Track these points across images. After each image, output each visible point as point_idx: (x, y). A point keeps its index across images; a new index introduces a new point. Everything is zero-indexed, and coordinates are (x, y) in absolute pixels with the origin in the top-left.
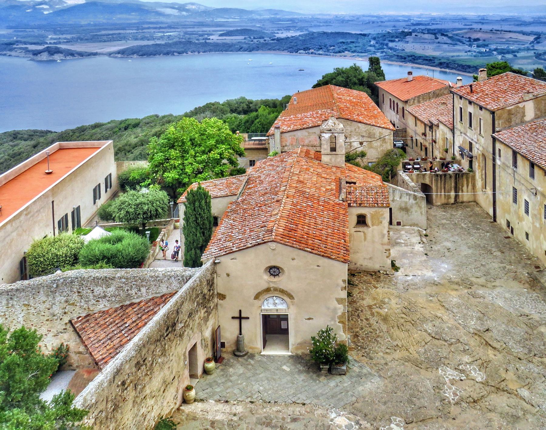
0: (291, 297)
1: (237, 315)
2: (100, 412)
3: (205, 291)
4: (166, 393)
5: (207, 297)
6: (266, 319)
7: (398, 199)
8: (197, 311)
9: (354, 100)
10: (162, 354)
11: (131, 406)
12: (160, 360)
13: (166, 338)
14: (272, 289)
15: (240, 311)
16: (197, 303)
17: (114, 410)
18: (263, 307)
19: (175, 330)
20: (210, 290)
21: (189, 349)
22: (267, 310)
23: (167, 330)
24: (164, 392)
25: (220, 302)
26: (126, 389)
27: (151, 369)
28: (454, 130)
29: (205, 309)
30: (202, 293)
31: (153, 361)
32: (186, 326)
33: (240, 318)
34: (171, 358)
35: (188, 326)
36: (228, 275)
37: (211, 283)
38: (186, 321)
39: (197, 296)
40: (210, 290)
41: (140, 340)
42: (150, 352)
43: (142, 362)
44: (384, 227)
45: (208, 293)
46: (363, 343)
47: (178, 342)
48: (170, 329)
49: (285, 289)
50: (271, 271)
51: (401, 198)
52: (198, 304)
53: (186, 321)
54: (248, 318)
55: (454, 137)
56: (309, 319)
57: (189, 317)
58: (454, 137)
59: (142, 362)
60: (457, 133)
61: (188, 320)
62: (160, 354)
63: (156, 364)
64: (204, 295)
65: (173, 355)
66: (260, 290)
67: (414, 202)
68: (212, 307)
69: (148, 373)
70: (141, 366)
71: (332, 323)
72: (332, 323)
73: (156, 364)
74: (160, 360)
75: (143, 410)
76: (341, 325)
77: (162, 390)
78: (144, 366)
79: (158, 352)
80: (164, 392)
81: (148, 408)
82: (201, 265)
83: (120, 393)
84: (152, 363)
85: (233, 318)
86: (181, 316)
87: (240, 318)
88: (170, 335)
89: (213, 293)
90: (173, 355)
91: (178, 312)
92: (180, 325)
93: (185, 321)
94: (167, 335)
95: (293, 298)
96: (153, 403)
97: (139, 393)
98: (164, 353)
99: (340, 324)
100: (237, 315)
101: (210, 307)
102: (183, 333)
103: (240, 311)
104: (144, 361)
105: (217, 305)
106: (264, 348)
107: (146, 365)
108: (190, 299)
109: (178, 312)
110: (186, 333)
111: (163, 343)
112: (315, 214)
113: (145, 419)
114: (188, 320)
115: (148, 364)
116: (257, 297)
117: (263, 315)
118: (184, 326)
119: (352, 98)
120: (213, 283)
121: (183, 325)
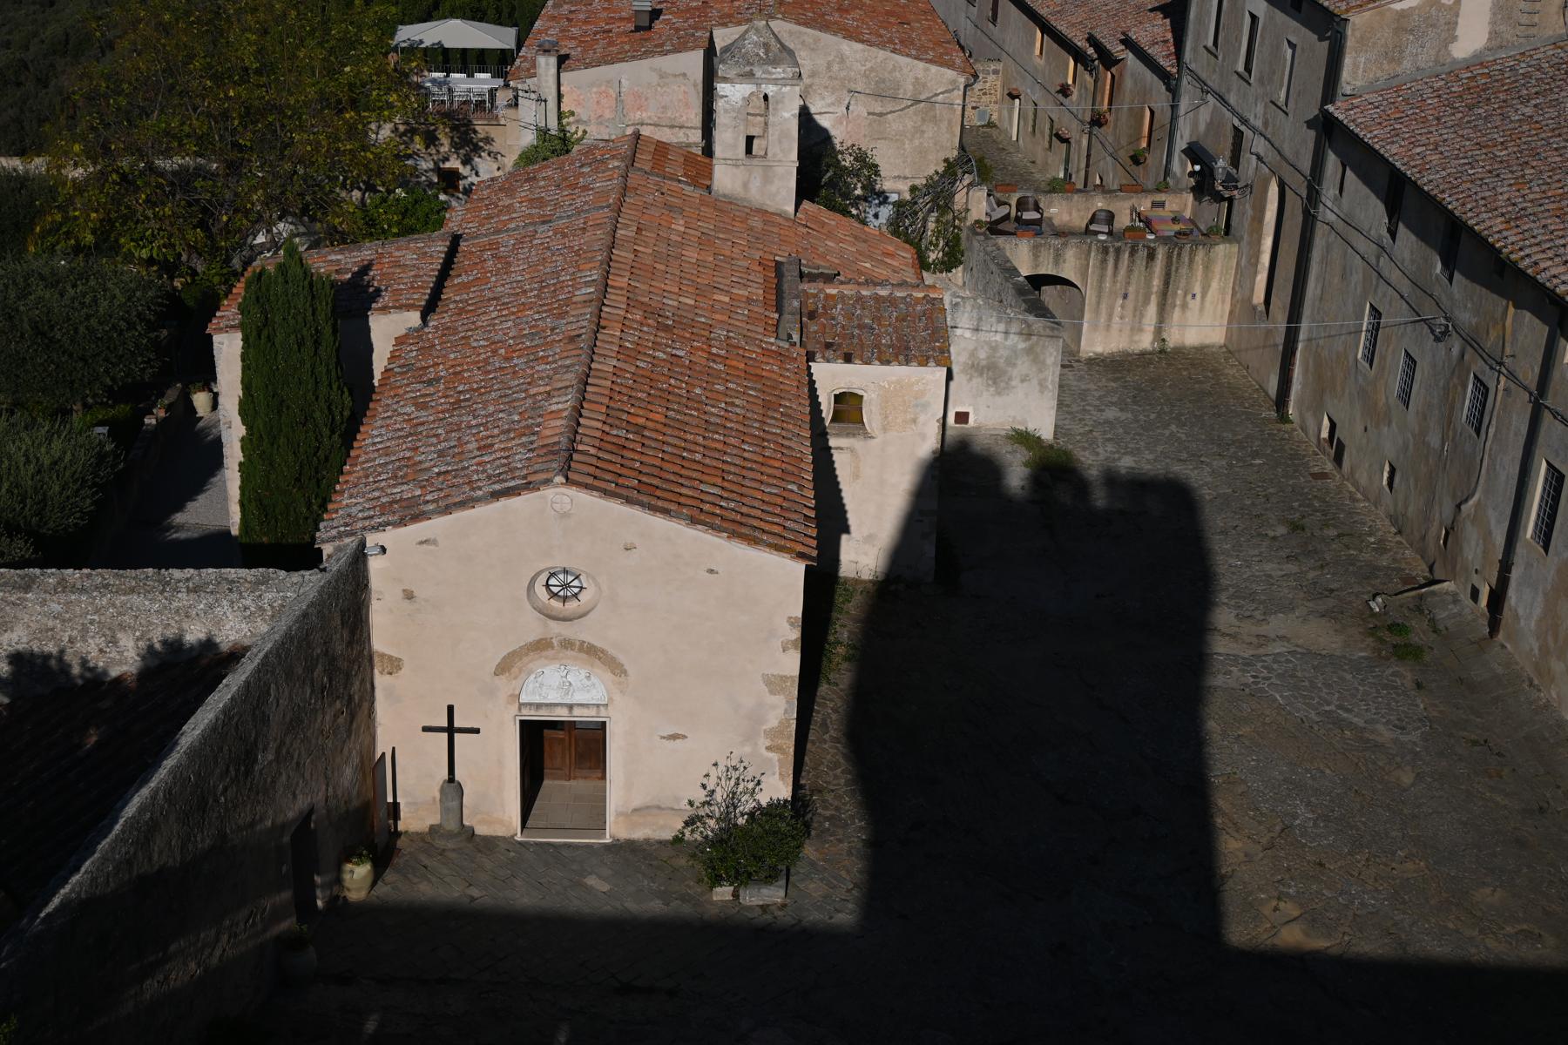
0: (615, 667)
6: (535, 736)
14: (555, 641)
18: (524, 699)
22: (539, 706)
33: (451, 730)
36: (409, 596)
38: (282, 743)
40: (350, 644)
44: (923, 437)
46: (837, 809)
49: (598, 644)
50: (553, 581)
56: (674, 737)
66: (515, 647)
71: (748, 749)
72: (748, 749)
76: (774, 756)
87: (451, 730)
95: (625, 672)
99: (771, 755)
103: (451, 709)
112: (698, 391)
116: (504, 668)
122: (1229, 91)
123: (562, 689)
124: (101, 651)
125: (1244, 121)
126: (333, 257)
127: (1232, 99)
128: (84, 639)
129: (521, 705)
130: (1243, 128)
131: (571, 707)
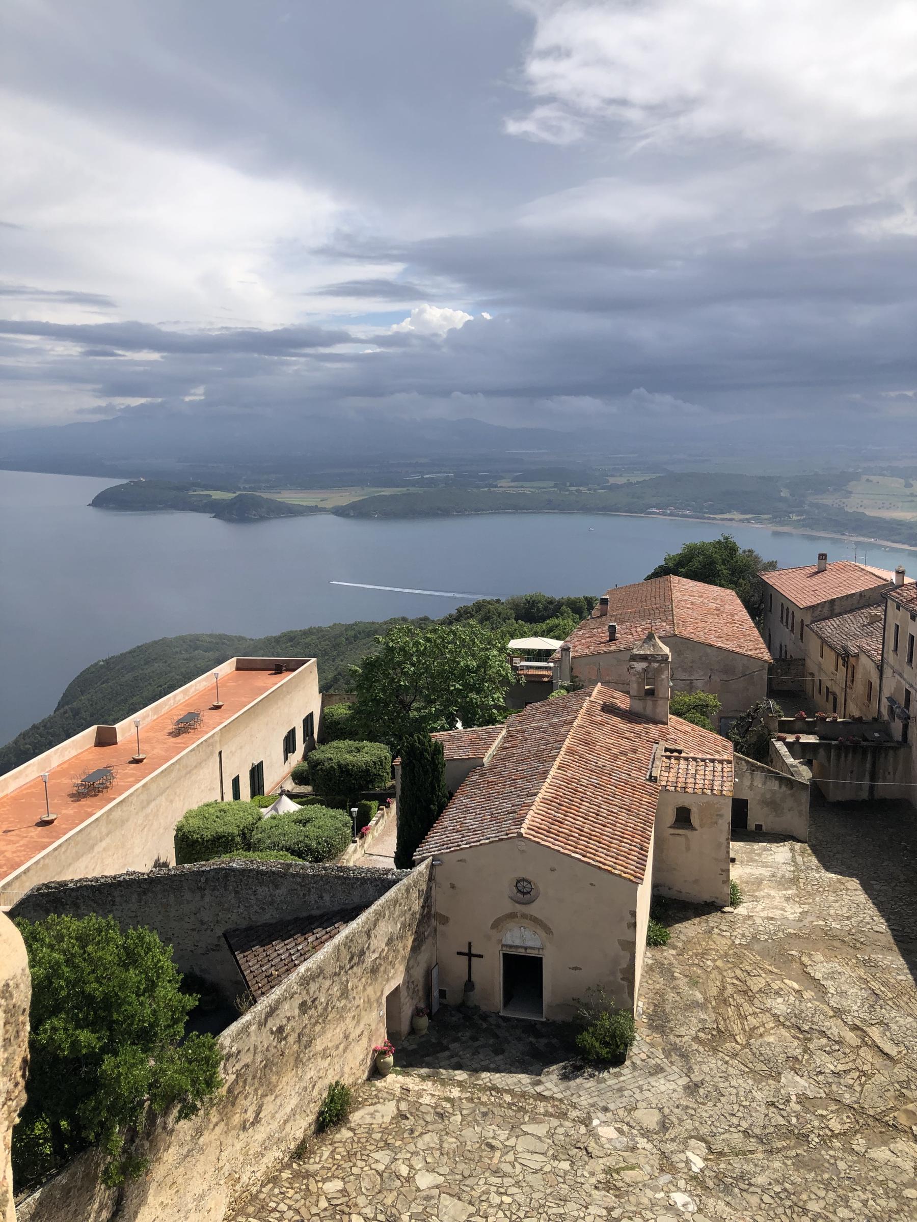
1: (466, 951)
2: (245, 1065)
4: (348, 1055)
7: (760, 786)
11: (292, 1064)
13: (350, 972)
15: (470, 944)
17: (266, 1066)
19: (363, 962)
21: (387, 993)
23: (350, 960)
24: (344, 1051)
25: (440, 928)
26: (285, 1039)
27: (324, 1016)
30: (410, 909)
38: (383, 950)
41: (308, 970)
42: (323, 991)
43: (309, 1003)
48: (356, 959)
51: (764, 784)
53: (383, 950)
54: (481, 956)
55: (881, 680)
57: (387, 945)
58: (881, 680)
59: (309, 1003)
60: (888, 672)
63: (333, 1008)
70: (310, 1008)
73: (333, 1008)
75: (312, 1073)
77: (342, 1047)
79: (336, 990)
80: (344, 1051)
81: (319, 1072)
82: (412, 865)
83: (275, 1044)
85: (459, 953)
86: (374, 943)
87: (470, 955)
91: (369, 936)
94: (352, 968)
96: (326, 1065)
100: (466, 951)
103: (470, 944)
104: (313, 1002)
105: (435, 930)
106: (505, 1006)
107: (316, 1007)
108: (389, 916)
111: (344, 979)
113: (314, 1087)
114: (386, 949)
115: (320, 1008)
117: (505, 955)
118: (379, 957)
123: (522, 938)
125: (911, 686)
129: (503, 946)
131: (526, 948)
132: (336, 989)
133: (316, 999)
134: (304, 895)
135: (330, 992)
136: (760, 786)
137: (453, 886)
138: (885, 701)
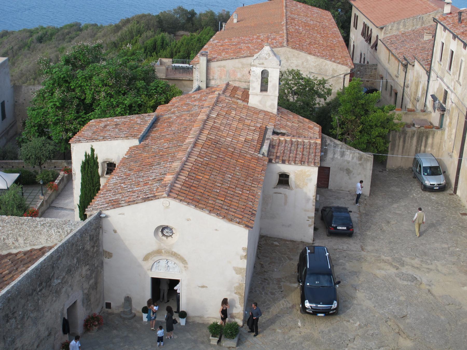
3: (88, 247)
5: (90, 254)
8: (78, 268)
9: (312, 23)
10: (35, 309)
12: (32, 315)
16: (77, 259)
19: (50, 286)
20: (93, 247)
28: (430, 73)
29: (88, 267)
31: (24, 315)
32: (64, 282)
34: (46, 314)
35: (66, 282)
37: (95, 239)
39: (78, 252)
45: (92, 249)
47: (54, 299)
48: (44, 284)
52: (79, 261)
53: (64, 277)
61: (66, 276)
62: (32, 308)
63: (28, 318)
64: (87, 251)
65: (48, 310)
67: (358, 162)
68: (96, 265)
69: (19, 327)
70: (10, 319)
74: (32, 315)
78: (14, 320)
79: (30, 306)
80: (38, 347)
84: (23, 318)
88: (44, 290)
89: (97, 251)
90: (48, 310)
91: (53, 267)
92: (56, 282)
93: (61, 277)
94: (41, 290)
97: (9, 345)
98: (37, 308)
101: (94, 265)
102: (60, 290)
107: (16, 318)
109: (53, 267)
110: (64, 290)
115: (18, 318)
118: (62, 282)
119: (309, 19)
120: (98, 239)
121: (59, 281)
122: (444, 77)
124: (13, 243)
126: (115, 120)
127: (445, 80)
128: (8, 239)
130: (447, 90)
132: (29, 305)
133: (15, 312)
134: (4, 239)
135: (25, 307)
136: (339, 158)
137: (115, 231)
138: (430, 98)
